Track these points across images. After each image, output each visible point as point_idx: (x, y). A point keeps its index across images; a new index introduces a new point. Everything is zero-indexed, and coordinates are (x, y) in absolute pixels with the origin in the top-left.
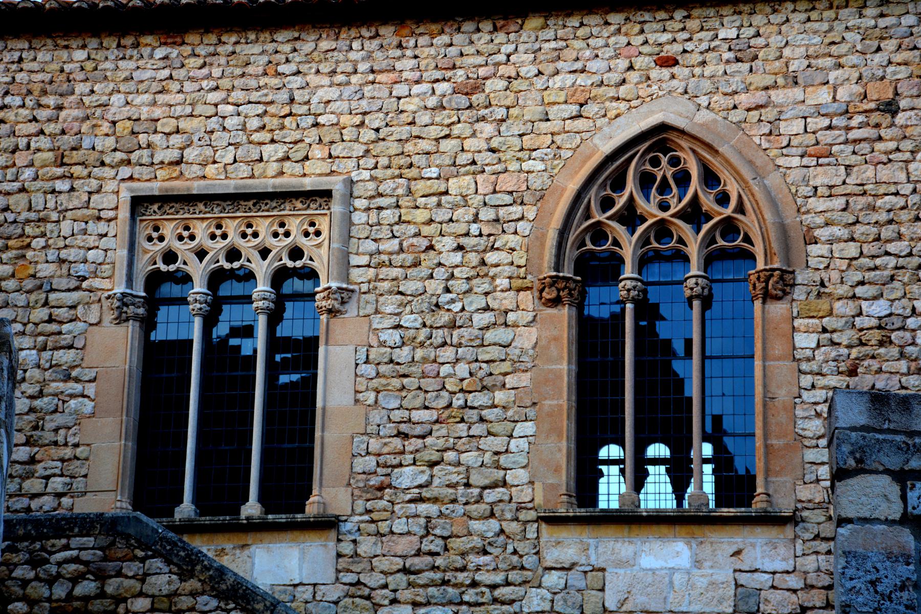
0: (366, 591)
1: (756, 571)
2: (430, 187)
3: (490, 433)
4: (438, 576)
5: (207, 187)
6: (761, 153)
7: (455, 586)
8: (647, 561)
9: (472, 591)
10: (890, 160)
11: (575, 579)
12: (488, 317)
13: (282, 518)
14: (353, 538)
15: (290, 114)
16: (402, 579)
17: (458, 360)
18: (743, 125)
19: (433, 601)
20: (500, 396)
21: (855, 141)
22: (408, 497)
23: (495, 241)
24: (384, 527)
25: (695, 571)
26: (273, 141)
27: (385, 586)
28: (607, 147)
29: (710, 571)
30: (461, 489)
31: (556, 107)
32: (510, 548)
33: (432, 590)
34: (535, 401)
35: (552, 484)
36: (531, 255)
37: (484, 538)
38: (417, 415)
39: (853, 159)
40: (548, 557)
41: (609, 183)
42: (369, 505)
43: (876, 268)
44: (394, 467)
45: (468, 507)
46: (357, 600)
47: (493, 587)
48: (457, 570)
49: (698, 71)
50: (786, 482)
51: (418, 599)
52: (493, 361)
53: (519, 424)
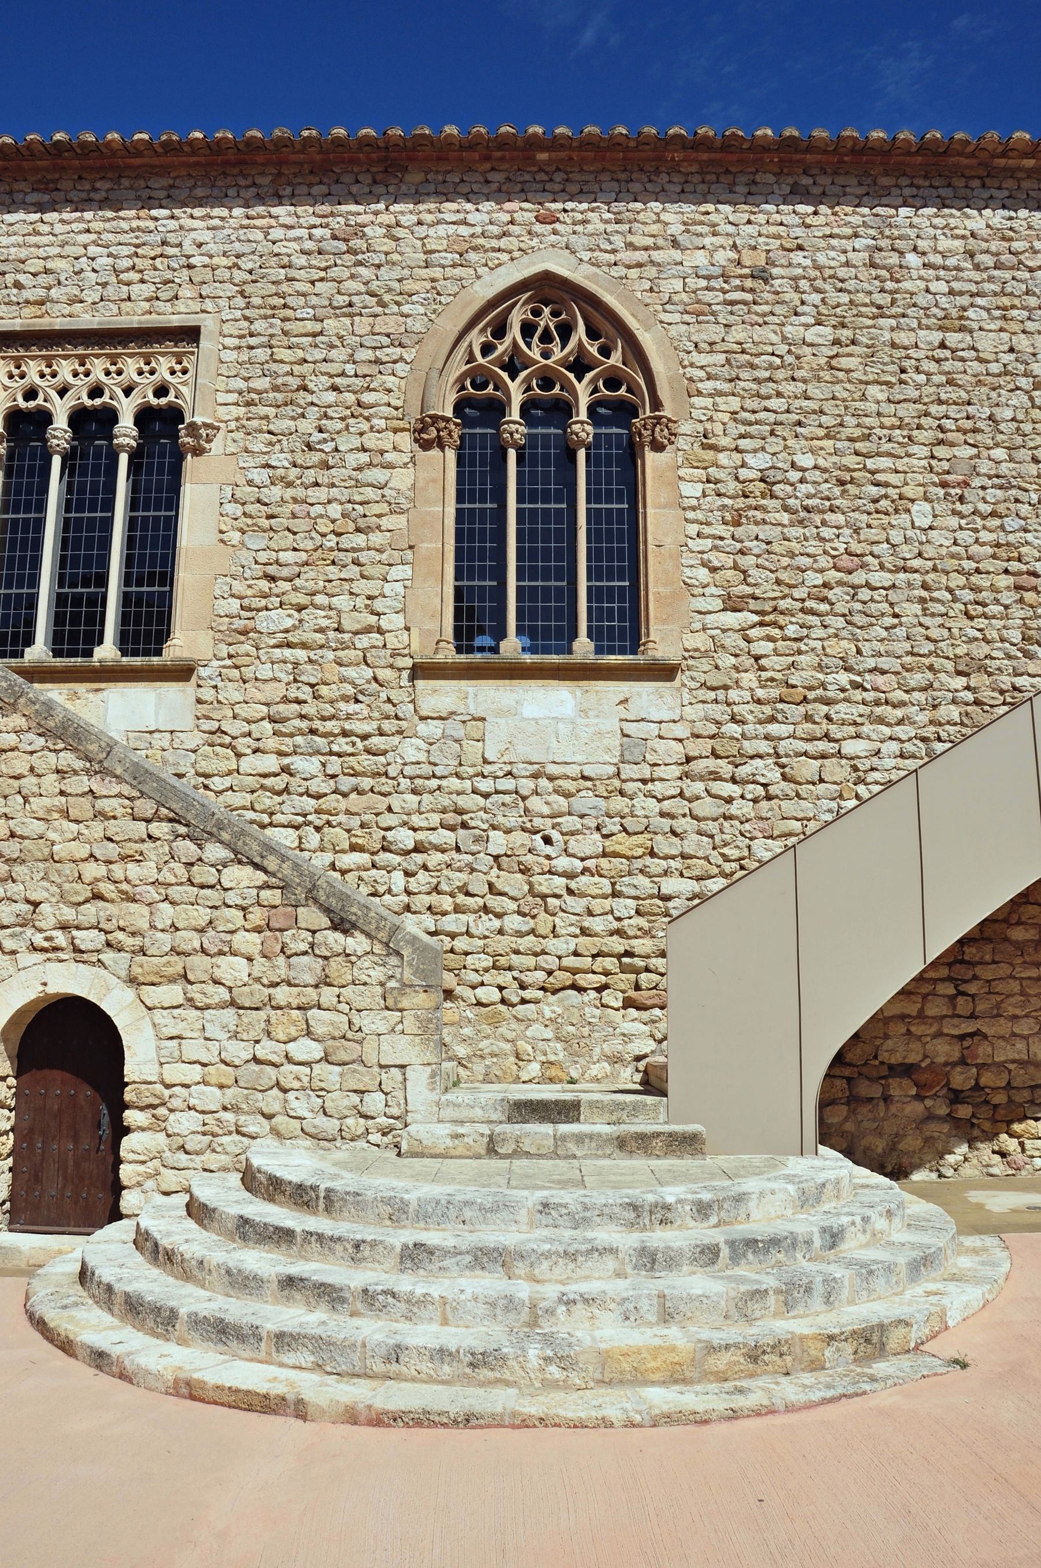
0: (227, 740)
1: (643, 720)
2: (304, 327)
3: (363, 577)
4: (304, 725)
5: (69, 323)
7: (325, 735)
8: (529, 710)
9: (342, 740)
10: (765, 323)
11: (454, 728)
12: (364, 458)
13: (138, 661)
14: (214, 683)
15: (161, 255)
16: (267, 727)
17: (329, 502)
19: (299, 750)
20: (377, 539)
21: (732, 303)
22: (272, 642)
24: (248, 672)
25: (579, 720)
26: (142, 281)
27: (249, 734)
28: (490, 293)
29: (596, 721)
30: (332, 634)
31: (437, 255)
32: (383, 696)
33: (299, 740)
35: (429, 630)
36: (408, 395)
37: (355, 685)
38: (286, 557)
39: (732, 319)
40: (423, 706)
41: (489, 330)
42: (232, 650)
43: (757, 423)
44: (258, 610)
45: (340, 653)
46: (218, 749)
47: (365, 737)
48: (324, 719)
49: (579, 228)
51: (284, 748)
52: (368, 503)
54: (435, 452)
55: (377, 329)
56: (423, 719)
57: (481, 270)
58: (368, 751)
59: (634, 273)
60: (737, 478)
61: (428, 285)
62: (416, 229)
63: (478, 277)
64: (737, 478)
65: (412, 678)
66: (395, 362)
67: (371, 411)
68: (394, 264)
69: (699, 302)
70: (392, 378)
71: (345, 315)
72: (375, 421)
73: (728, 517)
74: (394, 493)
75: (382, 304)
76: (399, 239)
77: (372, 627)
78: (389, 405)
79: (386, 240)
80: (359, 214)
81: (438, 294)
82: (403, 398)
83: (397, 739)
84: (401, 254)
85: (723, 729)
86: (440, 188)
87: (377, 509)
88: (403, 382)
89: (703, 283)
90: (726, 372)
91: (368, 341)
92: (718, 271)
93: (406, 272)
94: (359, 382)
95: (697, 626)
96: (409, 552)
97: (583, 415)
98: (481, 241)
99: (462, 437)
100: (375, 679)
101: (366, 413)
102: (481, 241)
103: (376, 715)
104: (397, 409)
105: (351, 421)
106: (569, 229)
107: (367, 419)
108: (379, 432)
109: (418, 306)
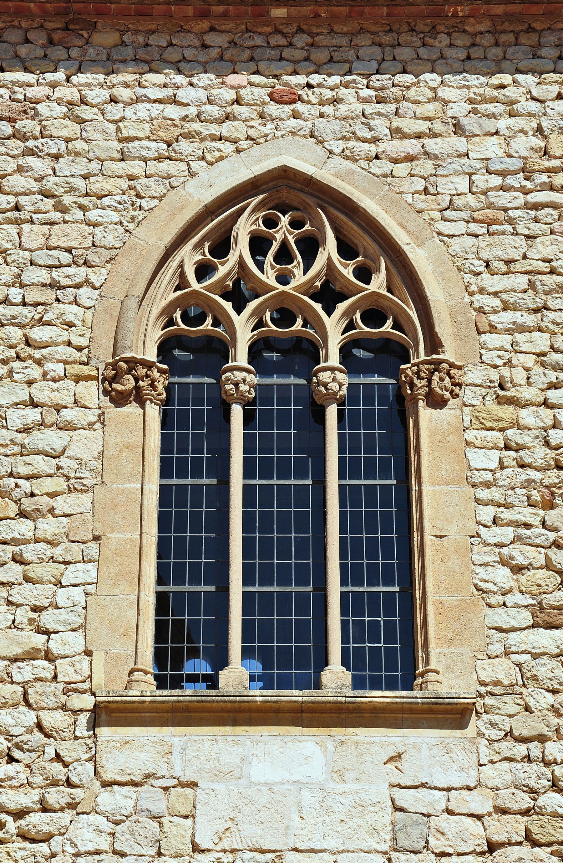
1: (423, 785)
3: (27, 579)
6: (415, 215)
12: (33, 415)
18: (389, 180)
21: (537, 207)
23: (46, 311)
29: (355, 786)
31: (136, 143)
32: (50, 752)
34: (97, 533)
35: (119, 655)
37: (9, 736)
39: (536, 228)
41: (207, 245)
47: (19, 814)
49: (328, 110)
50: (461, 655)
52: (36, 477)
53: (70, 567)
54: (132, 409)
55: (54, 242)
56: (106, 784)
57: (196, 166)
58: (24, 836)
59: (402, 169)
60: (547, 443)
61: (124, 184)
62: (109, 108)
63: (192, 175)
64: (547, 443)
65: (93, 725)
66: (78, 286)
67: (45, 352)
68: (77, 154)
69: (490, 206)
70: (74, 308)
71: (10, 222)
72: (49, 366)
73: (536, 496)
74: (74, 464)
75: (62, 208)
76: (84, 121)
77: (39, 650)
78: (69, 344)
79: (67, 122)
80: (30, 86)
81: (138, 196)
82: (88, 335)
83: (66, 816)
84: (88, 141)
85: (541, 801)
86: (141, 54)
87: (49, 485)
88: (89, 313)
89: (497, 181)
90: (530, 300)
91: (42, 257)
92: (516, 164)
93: (95, 166)
94: (27, 313)
95: (497, 649)
96: (93, 545)
97: (334, 359)
98: (196, 126)
99: (169, 389)
100: (40, 726)
101: (37, 354)
102: (196, 126)
103: (38, 780)
104: (80, 349)
105: (17, 365)
106: (315, 111)
107: (39, 363)
108: (54, 380)
109: (109, 212)
